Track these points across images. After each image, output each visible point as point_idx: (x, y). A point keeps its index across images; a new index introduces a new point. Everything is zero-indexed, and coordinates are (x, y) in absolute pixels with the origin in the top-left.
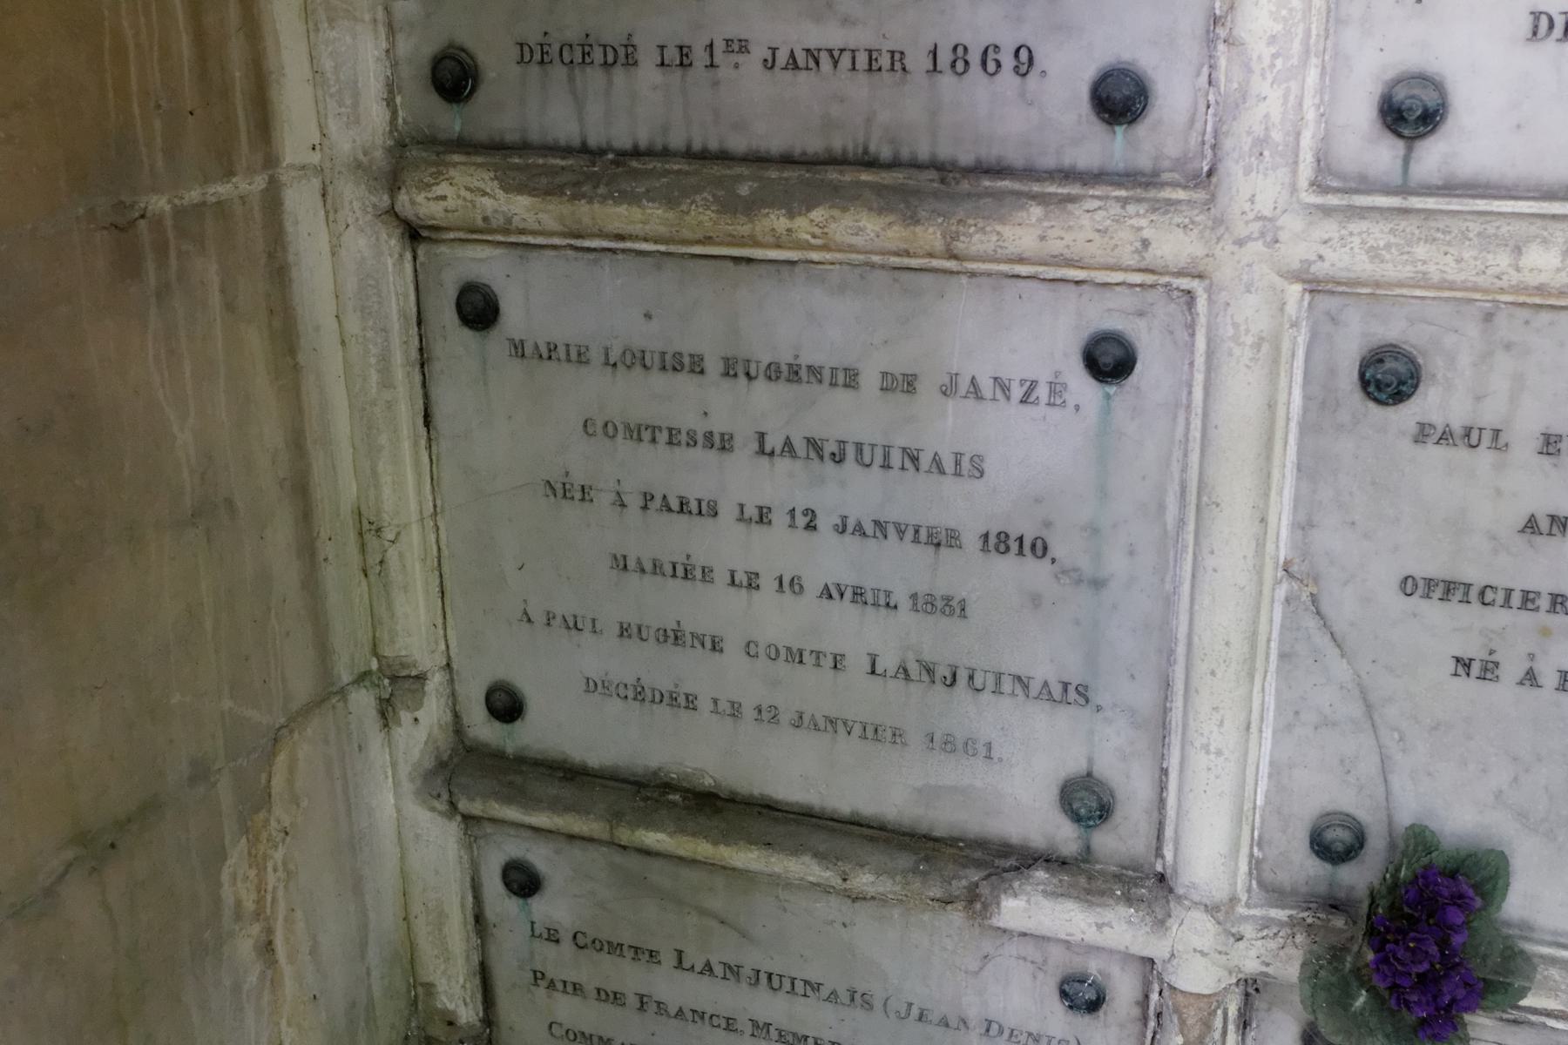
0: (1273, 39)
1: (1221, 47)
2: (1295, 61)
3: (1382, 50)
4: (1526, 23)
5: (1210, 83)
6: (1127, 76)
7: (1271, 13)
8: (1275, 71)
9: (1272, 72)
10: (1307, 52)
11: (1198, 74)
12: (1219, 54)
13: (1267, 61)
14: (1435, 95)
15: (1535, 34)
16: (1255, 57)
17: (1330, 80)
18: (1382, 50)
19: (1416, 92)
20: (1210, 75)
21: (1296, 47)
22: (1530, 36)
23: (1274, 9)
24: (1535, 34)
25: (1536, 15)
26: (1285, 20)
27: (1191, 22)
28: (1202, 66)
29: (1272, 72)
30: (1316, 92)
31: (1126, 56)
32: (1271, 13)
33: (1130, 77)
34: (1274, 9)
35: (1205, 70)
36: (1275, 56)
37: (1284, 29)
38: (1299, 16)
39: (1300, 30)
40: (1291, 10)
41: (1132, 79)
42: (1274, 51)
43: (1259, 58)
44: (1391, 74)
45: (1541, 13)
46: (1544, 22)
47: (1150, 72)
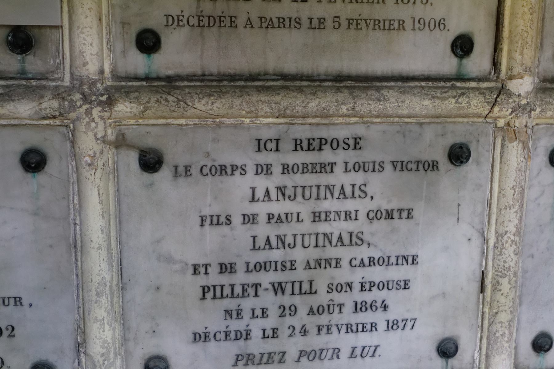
0: (102, 355)
1: (82, 355)
2: (112, 360)
3: (143, 349)
4: (192, 337)
5: (79, 365)
6: (45, 366)
7: (101, 346)
8: (105, 365)
9: (104, 366)
10: (115, 354)
11: (74, 362)
12: (82, 357)
13: (101, 362)
14: (164, 364)
15: (195, 339)
16: (96, 361)
17: (125, 361)
18: (143, 349)
19: (157, 364)
20: (79, 362)
21: (112, 355)
22: (194, 341)
23: (102, 345)
24: (195, 339)
25: (195, 334)
26: (106, 348)
27: (69, 344)
28: (75, 359)
29: (104, 366)
30: (121, 367)
31: (44, 358)
32: (101, 346)
33: (46, 367)
34: (102, 345)
35: (77, 361)
36: (104, 360)
37: (106, 351)
38: (111, 345)
39: (112, 350)
40: (108, 344)
41: (48, 368)
42: (103, 359)
43: (98, 361)
44: (147, 357)
45: (196, 333)
46: (198, 335)
47: (54, 363)
